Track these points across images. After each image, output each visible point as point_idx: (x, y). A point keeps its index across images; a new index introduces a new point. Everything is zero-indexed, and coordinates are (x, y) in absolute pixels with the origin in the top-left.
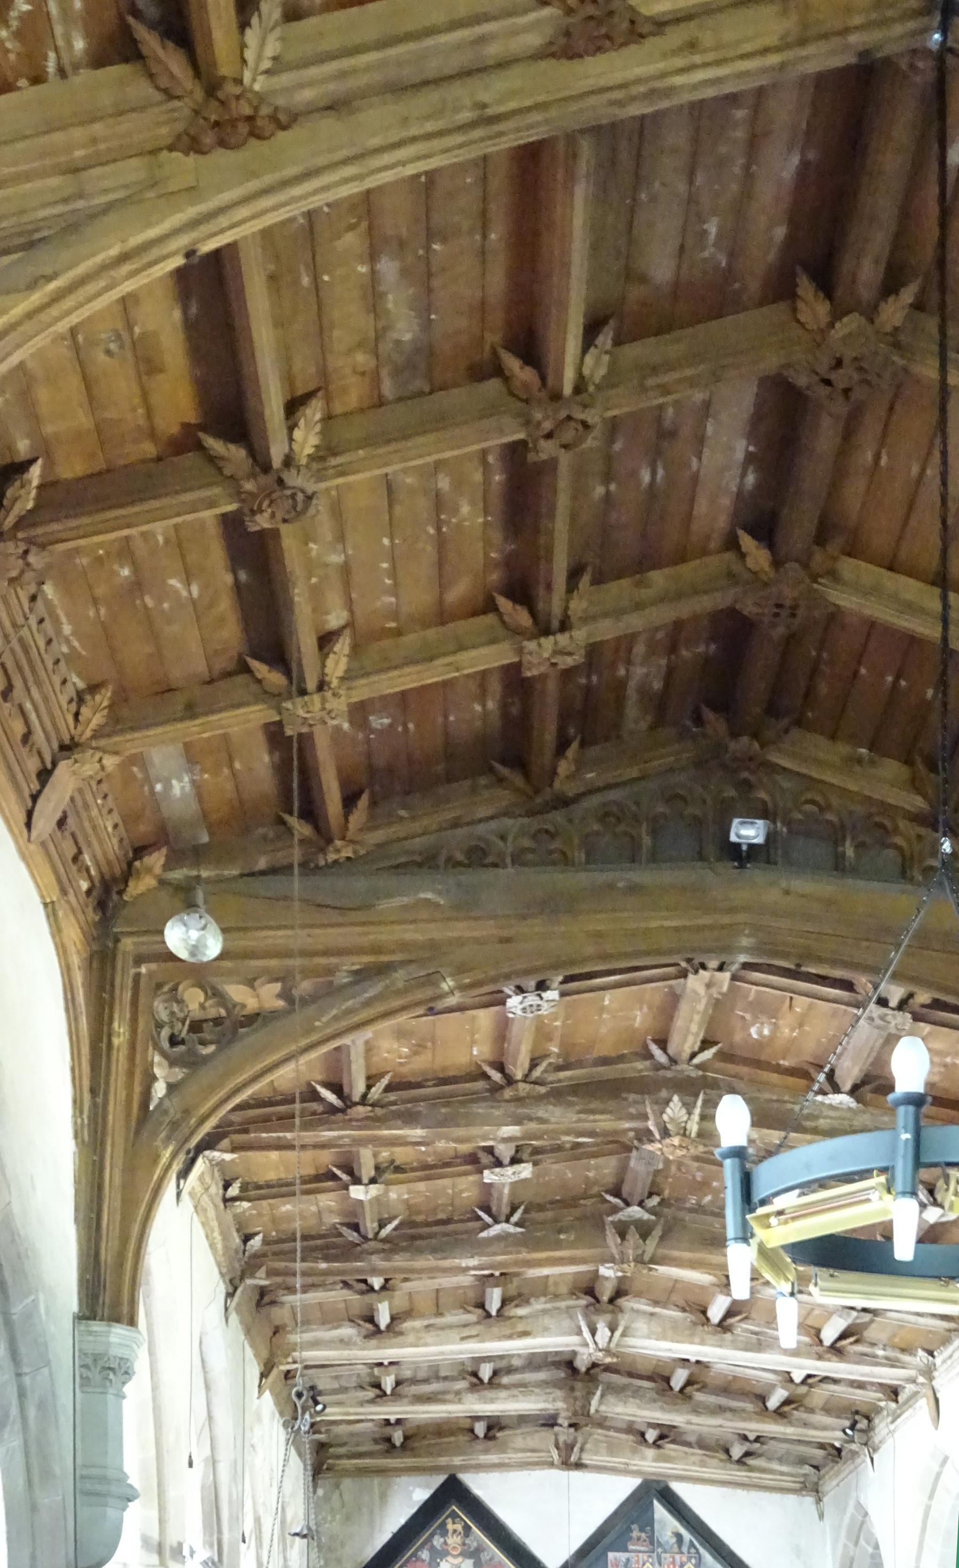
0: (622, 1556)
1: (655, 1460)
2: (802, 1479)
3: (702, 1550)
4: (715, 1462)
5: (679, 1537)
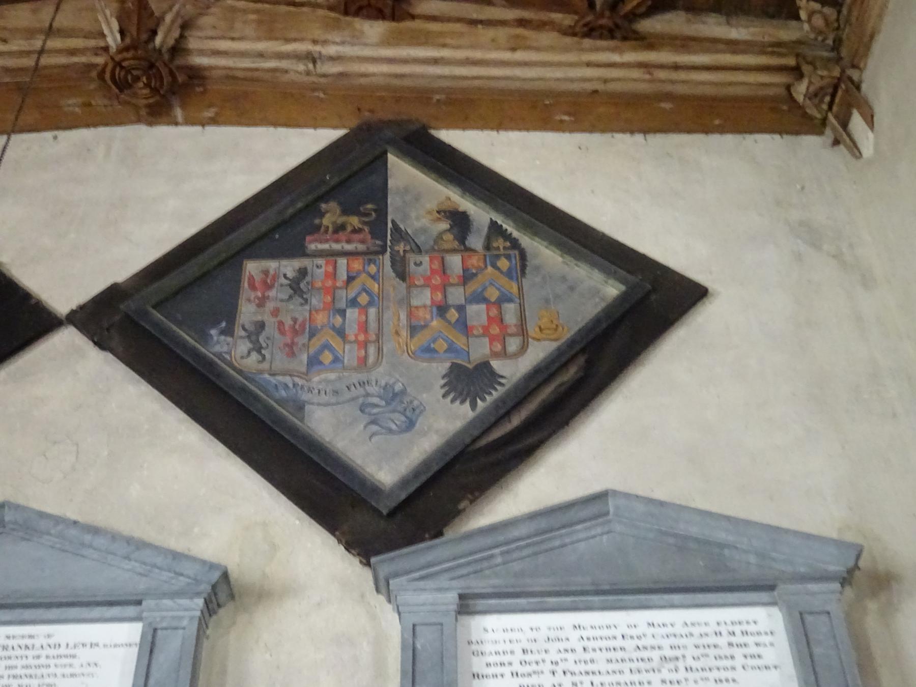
0: (289, 267)
1: (386, 42)
2: (791, 61)
3: (526, 241)
4: (547, 38)
5: (460, 222)
